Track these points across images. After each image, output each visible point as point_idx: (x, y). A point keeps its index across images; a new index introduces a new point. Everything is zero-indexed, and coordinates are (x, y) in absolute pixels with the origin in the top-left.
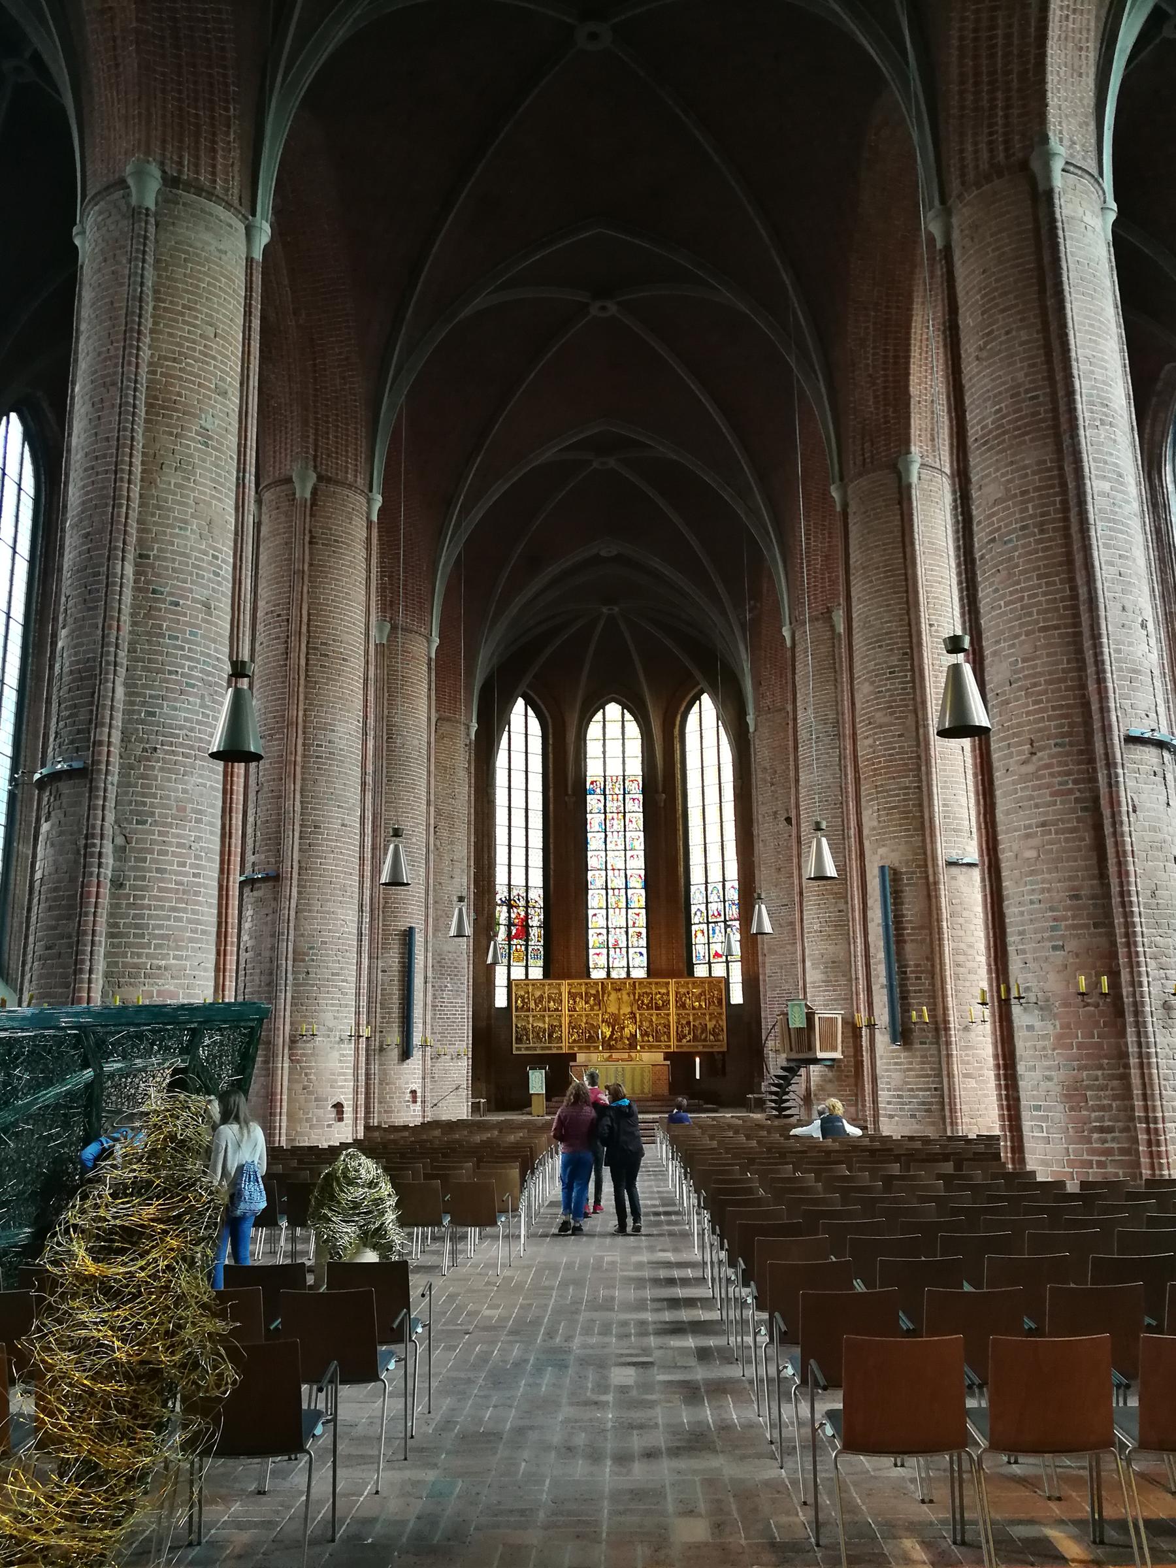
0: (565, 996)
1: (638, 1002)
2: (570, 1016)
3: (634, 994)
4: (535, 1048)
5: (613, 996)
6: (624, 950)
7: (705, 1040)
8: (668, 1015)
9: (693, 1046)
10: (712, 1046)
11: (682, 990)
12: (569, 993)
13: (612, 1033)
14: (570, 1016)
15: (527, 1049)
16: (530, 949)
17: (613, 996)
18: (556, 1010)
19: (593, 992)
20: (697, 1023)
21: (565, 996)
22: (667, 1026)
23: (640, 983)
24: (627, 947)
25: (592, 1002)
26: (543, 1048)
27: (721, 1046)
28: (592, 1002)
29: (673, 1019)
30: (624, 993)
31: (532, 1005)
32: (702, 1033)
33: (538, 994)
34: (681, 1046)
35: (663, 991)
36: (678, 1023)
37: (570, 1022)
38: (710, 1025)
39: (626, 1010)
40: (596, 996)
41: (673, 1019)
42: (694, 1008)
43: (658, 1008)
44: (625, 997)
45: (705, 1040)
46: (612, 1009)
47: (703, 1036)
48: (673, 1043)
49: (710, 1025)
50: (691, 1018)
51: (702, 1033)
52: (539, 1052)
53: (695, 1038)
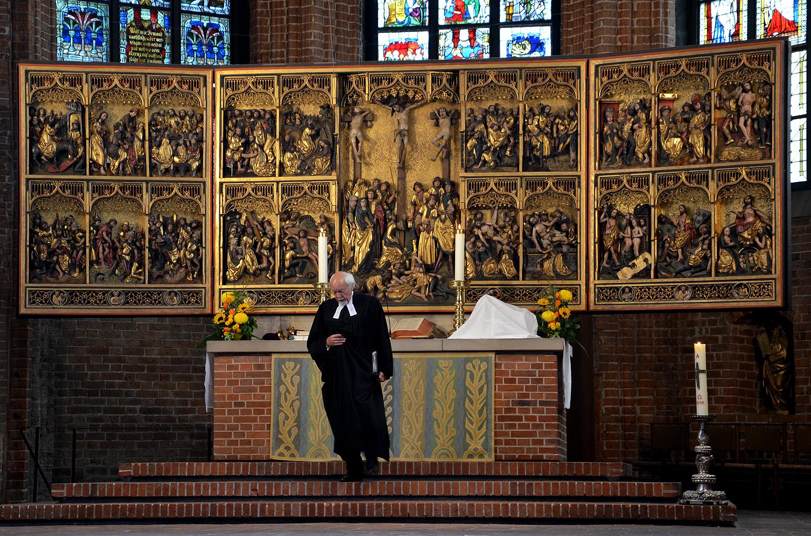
0: (215, 128)
1: (464, 143)
2: (232, 191)
3: (454, 118)
4: (103, 297)
5: (384, 126)
6: (483, 36)
7: (701, 268)
8: (571, 184)
9: (660, 292)
10: (726, 291)
11: (628, 99)
12: (229, 113)
13: (375, 252)
14: (232, 191)
15: (72, 297)
16: (186, 23)
17: (384, 126)
18: (182, 169)
19: (311, 110)
20: (673, 213)
21: (215, 128)
22: (566, 224)
23: (473, 77)
24: (494, 25)
25: (305, 145)
26: (129, 296)
27: (763, 289)
28: (305, 145)
29: (588, 197)
30: (423, 115)
31: (97, 154)
32: (690, 244)
33: (118, 113)
34: (617, 292)
35: (559, 103)
36: (606, 210)
37: (230, 216)
38: (721, 219)
39: (425, 171)
40: (318, 126)
41: (588, 197)
42: (663, 157)
43: (533, 161)
44: (424, 129)
45: (701, 268)
46: (380, 169)
47: (695, 256)
48: (589, 278)
49: (721, 219)
50: (653, 193)
51: (690, 244)
52: (114, 307)
53: (666, 263)
